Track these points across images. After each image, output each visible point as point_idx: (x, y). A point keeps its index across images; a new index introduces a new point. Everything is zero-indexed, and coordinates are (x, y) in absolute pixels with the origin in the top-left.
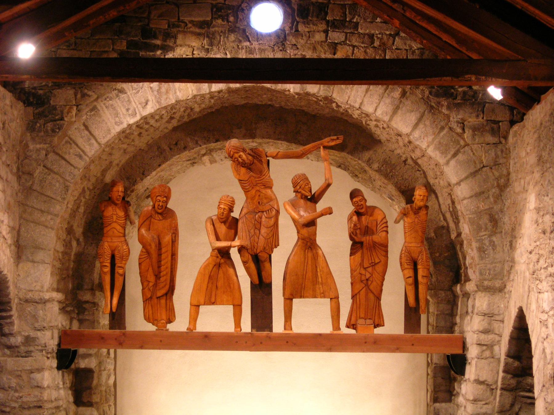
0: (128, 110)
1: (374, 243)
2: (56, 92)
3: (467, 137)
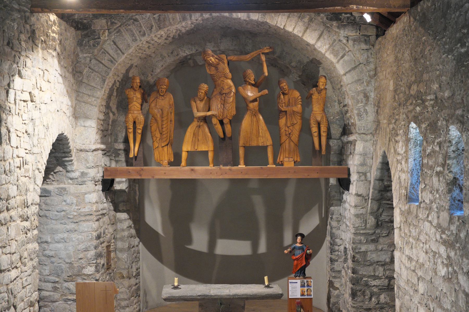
1: (294, 111)
2: (95, 21)
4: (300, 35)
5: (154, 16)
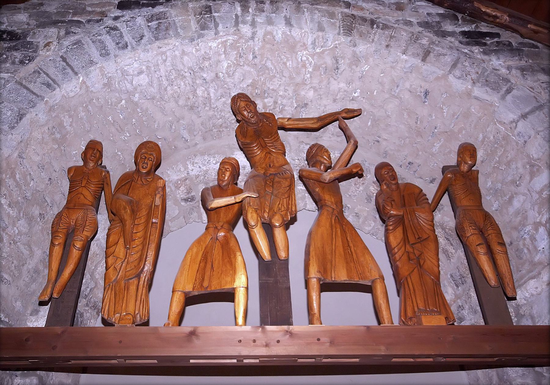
0: (117, 44)
5: (150, 24)
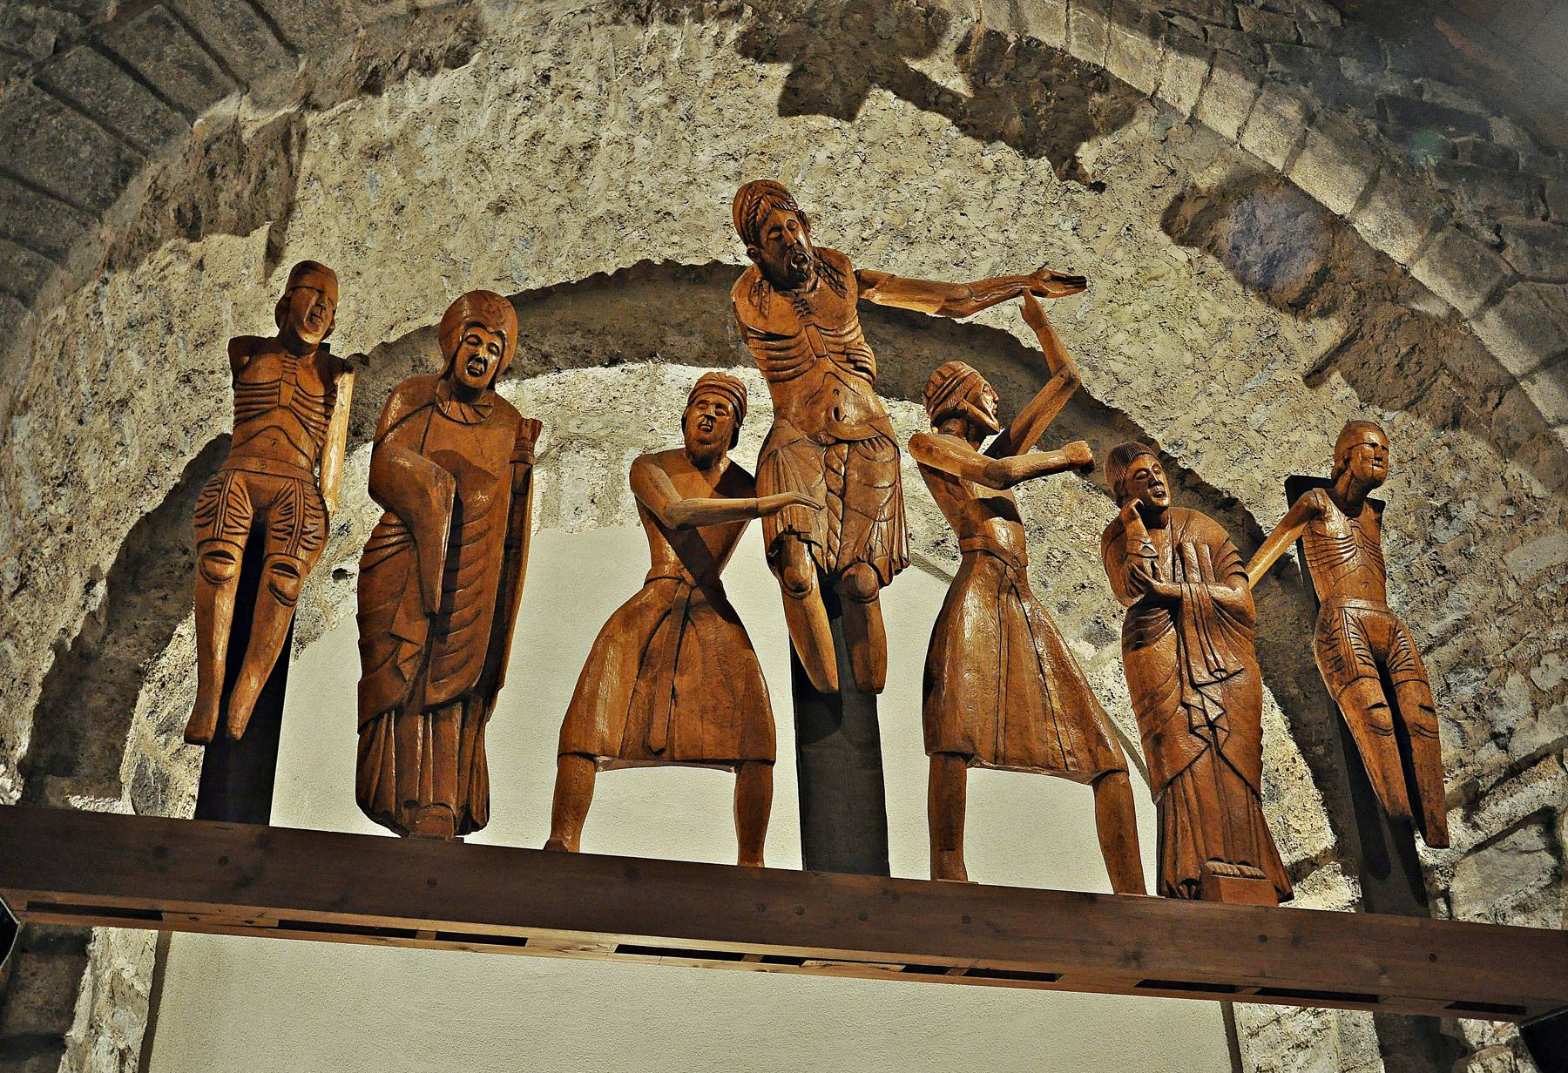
3: (1516, 257)
4: (1278, 163)
